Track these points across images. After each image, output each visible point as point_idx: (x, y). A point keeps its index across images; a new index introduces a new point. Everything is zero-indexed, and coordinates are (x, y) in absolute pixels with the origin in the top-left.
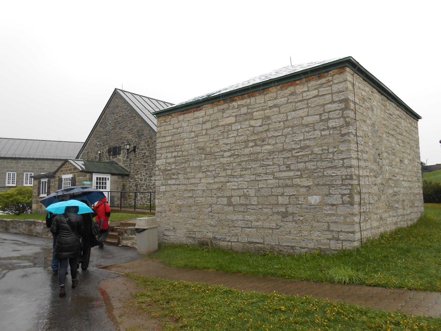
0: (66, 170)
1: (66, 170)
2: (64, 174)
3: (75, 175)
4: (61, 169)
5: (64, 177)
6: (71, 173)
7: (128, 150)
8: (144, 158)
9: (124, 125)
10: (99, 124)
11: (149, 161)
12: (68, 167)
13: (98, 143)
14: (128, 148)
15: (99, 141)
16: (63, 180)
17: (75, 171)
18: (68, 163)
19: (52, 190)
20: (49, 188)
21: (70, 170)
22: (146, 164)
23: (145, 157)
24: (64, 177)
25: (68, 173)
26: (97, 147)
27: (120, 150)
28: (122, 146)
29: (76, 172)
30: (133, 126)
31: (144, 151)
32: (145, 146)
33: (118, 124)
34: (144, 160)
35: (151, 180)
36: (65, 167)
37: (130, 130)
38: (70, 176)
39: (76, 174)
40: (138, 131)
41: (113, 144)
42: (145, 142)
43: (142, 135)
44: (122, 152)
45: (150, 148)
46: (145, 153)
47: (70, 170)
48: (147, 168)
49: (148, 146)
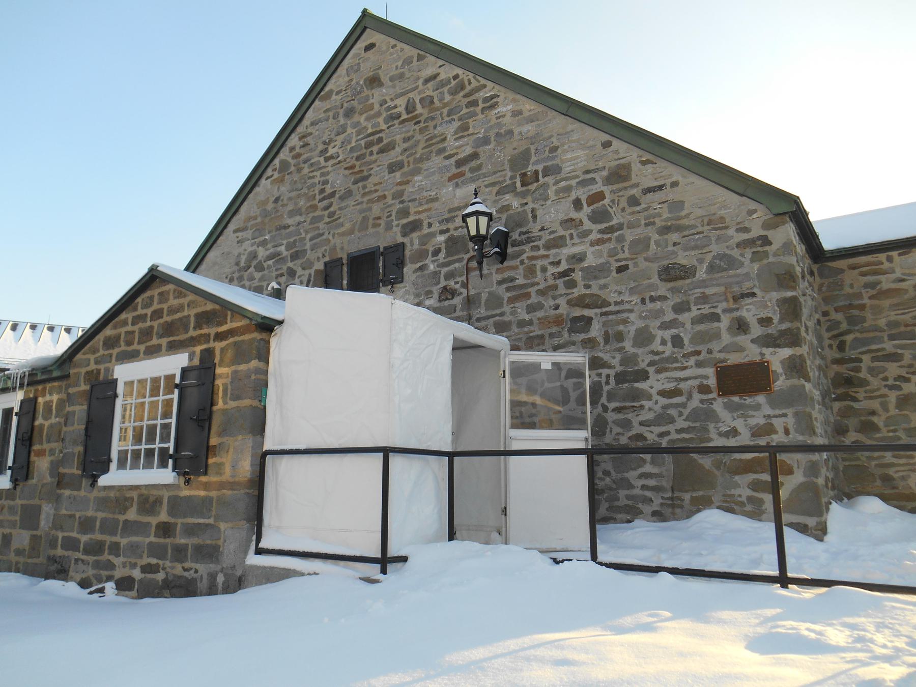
0: (146, 334)
1: (146, 334)
2: (130, 356)
3: (208, 355)
4: (108, 332)
5: (124, 373)
6: (174, 347)
7: (479, 239)
8: (572, 284)
9: (420, 151)
10: (269, 172)
11: (613, 297)
12: (157, 314)
13: (262, 253)
14: (483, 231)
15: (264, 243)
16: (120, 389)
17: (213, 331)
18: (154, 292)
19: (41, 453)
20: (27, 440)
21: (168, 329)
22: (587, 312)
23: (578, 276)
24: (124, 373)
25: (153, 352)
26: (260, 268)
27: (401, 264)
28: (413, 243)
29: (219, 337)
30: (486, 141)
31: (566, 251)
32: (568, 222)
33: (381, 151)
34: (578, 291)
35: (637, 395)
36: (137, 320)
37: (459, 164)
38: (174, 364)
39: (218, 346)
40: (520, 161)
41: (347, 244)
42: (577, 204)
43: (547, 172)
44: (409, 270)
45: (611, 230)
46: (579, 258)
47: (168, 329)
48: (596, 331)
49: (599, 216)
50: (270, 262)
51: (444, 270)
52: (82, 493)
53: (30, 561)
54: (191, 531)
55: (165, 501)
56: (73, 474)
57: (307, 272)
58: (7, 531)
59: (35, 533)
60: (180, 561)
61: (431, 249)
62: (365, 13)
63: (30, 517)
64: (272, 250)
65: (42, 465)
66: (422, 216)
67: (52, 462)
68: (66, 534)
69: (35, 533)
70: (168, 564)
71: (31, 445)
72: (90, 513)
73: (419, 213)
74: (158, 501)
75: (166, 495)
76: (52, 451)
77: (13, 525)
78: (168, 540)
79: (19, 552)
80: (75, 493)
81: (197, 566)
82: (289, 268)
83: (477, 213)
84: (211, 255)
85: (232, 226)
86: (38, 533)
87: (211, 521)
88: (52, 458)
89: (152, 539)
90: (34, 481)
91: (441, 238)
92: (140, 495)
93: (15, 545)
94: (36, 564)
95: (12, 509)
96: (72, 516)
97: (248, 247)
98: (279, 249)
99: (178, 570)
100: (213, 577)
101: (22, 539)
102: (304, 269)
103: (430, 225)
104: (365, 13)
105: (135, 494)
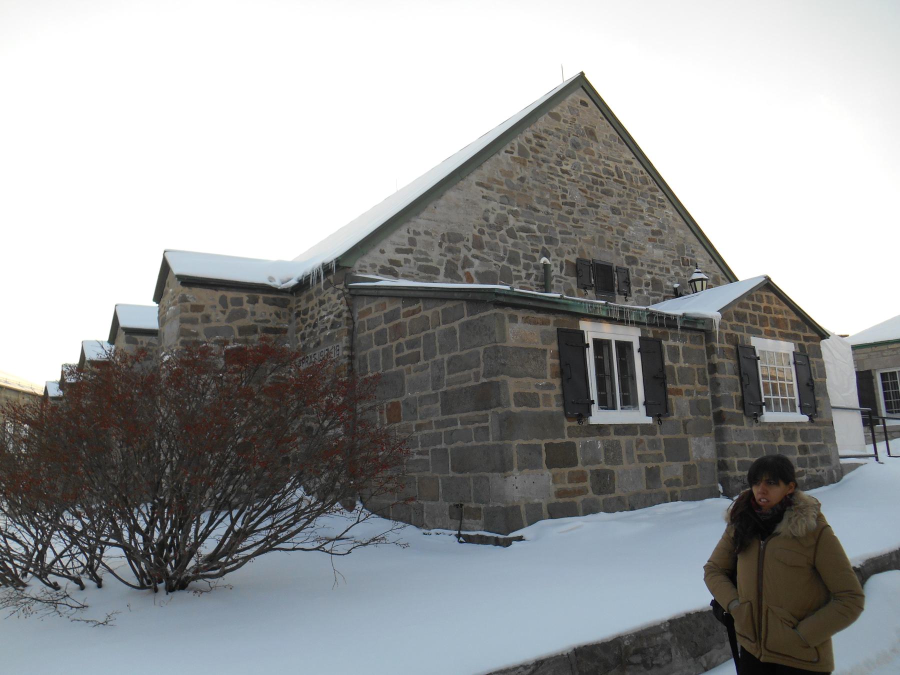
19: (678, 392)
26: (511, 233)
50: (524, 235)
51: (652, 298)
52: (746, 427)
53: (688, 488)
54: (816, 449)
55: (798, 432)
56: (734, 413)
57: (560, 259)
58: (650, 465)
59: (687, 463)
60: (813, 467)
61: (644, 281)
62: (582, 74)
63: (677, 450)
64: (523, 224)
65: (680, 404)
66: (637, 256)
67: (690, 402)
68: (741, 459)
69: (687, 463)
70: (808, 469)
71: (664, 385)
72: (755, 442)
73: (635, 253)
74: (795, 433)
75: (798, 429)
76: (689, 393)
77: (659, 458)
78: (806, 456)
79: (670, 483)
80: (741, 427)
81: (823, 468)
82: (544, 248)
83: (702, 280)
84: (451, 195)
85: (474, 178)
86: (691, 463)
87: (822, 443)
88: (690, 398)
89: (798, 455)
90: (675, 417)
91: (649, 276)
92: (784, 429)
93: (664, 477)
94: (696, 490)
95: (654, 444)
96: (742, 445)
97: (496, 208)
98: (531, 226)
99: (814, 472)
100: (830, 472)
101: (674, 470)
102: (558, 255)
103: (642, 265)
104: (582, 74)
105: (780, 428)
